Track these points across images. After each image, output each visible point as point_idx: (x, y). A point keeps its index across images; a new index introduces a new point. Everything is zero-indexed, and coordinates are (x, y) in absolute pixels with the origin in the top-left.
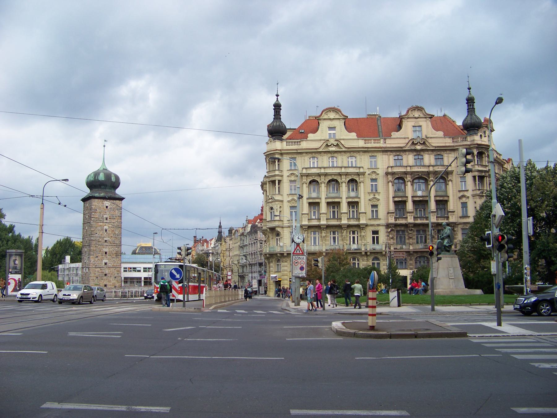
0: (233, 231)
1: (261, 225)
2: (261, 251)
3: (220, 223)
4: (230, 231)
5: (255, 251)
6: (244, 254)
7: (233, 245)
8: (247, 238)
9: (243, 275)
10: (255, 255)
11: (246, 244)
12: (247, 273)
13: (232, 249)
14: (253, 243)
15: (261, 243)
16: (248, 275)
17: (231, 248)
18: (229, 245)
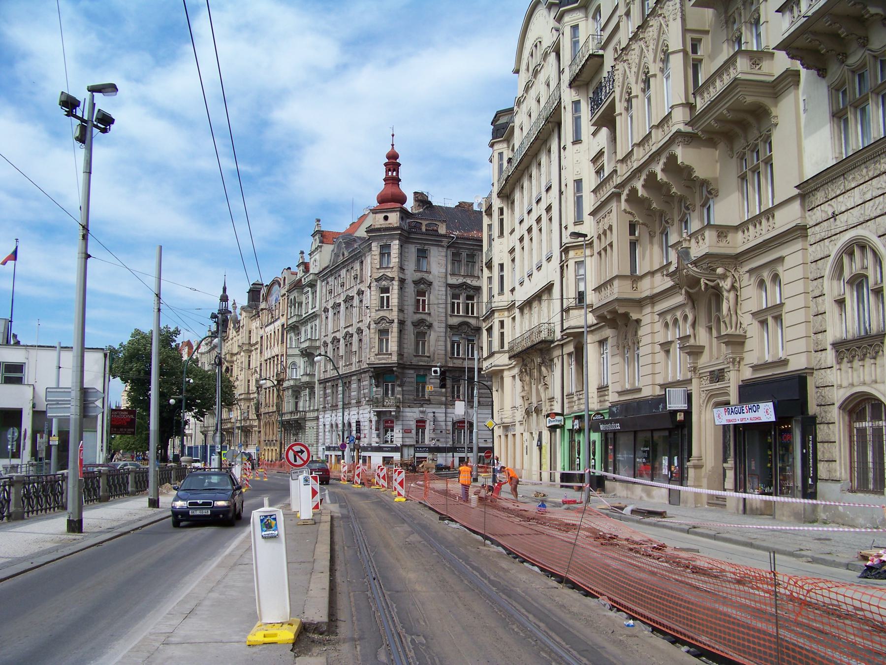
0: (263, 291)
1: (386, 218)
2: (383, 319)
3: (225, 289)
4: (254, 293)
5: (350, 329)
6: (304, 345)
7: (261, 332)
8: (314, 293)
9: (296, 421)
10: (348, 345)
11: (310, 312)
12: (314, 411)
13: (257, 343)
14: (340, 300)
15: (385, 290)
16: (317, 418)
17: (253, 341)
18: (250, 332)
